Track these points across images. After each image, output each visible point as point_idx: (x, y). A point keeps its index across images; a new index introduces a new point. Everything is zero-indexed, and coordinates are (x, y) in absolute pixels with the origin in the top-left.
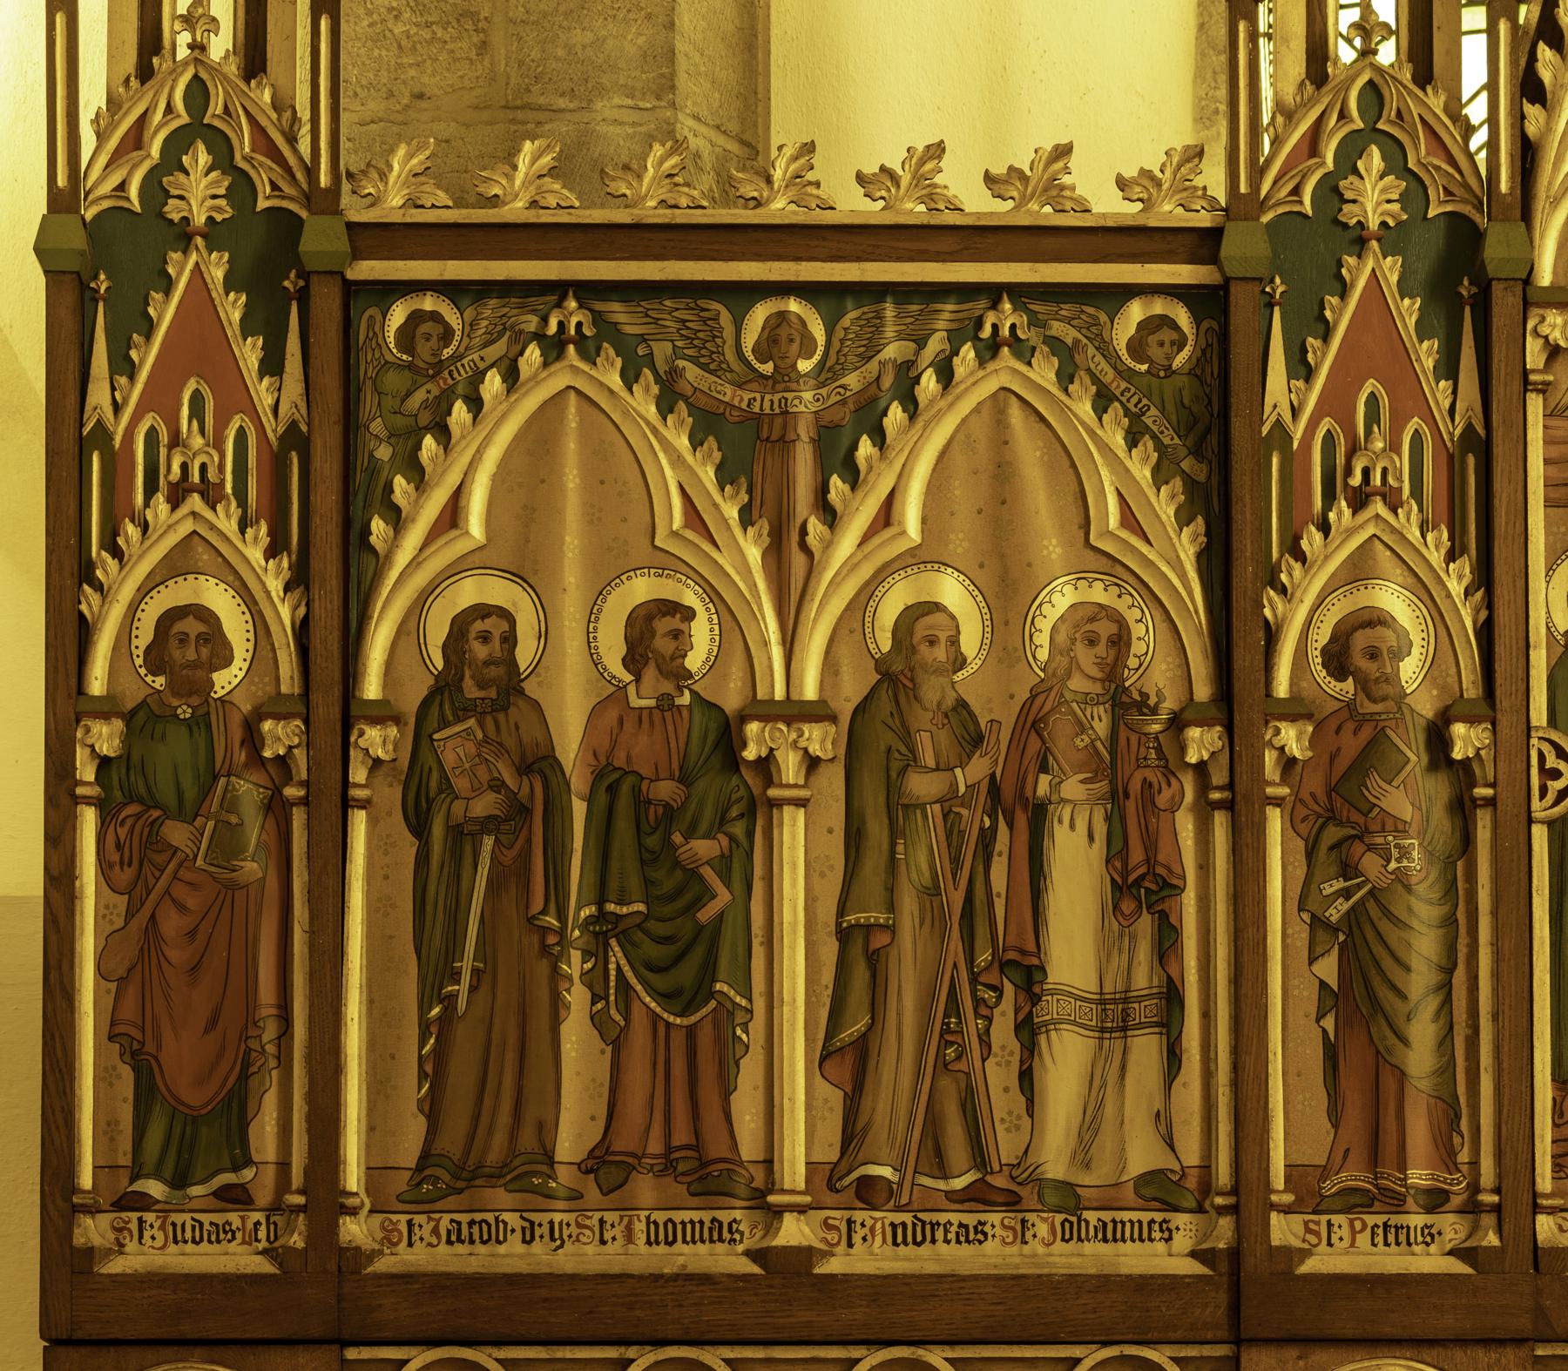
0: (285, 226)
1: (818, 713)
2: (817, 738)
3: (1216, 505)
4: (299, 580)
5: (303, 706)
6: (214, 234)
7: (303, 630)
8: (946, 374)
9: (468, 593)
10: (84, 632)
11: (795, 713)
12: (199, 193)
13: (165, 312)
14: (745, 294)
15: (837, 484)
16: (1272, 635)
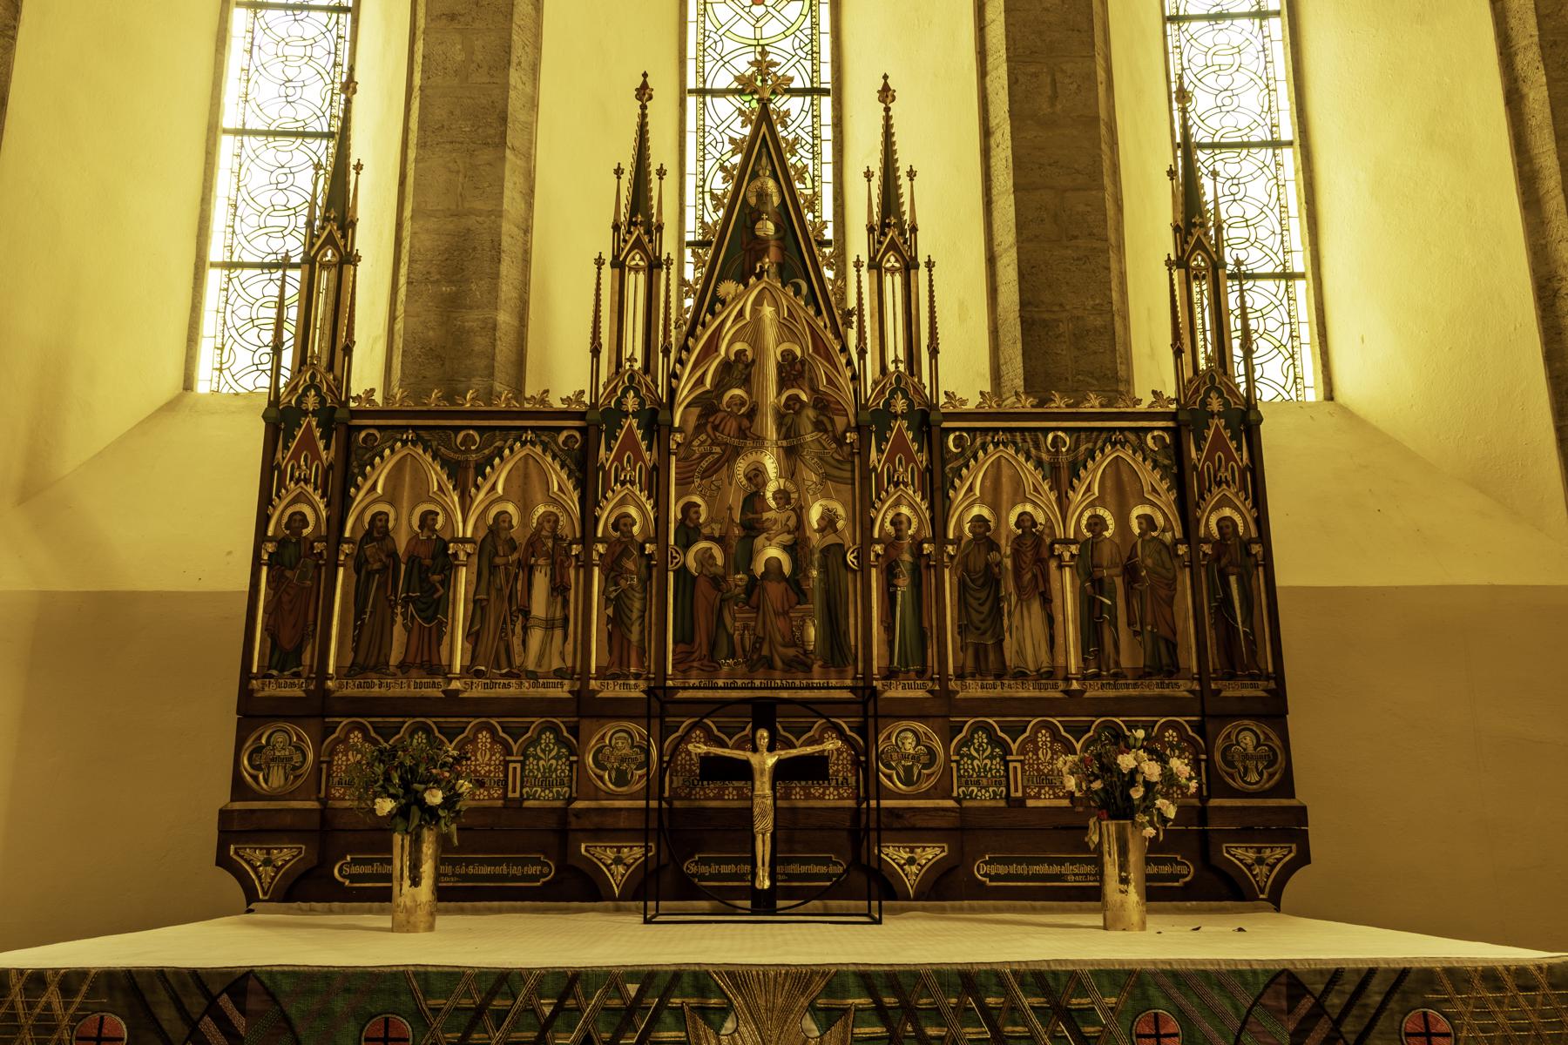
0: (925, 415)
1: (1074, 542)
2: (1074, 549)
3: (1180, 484)
4: (931, 507)
5: (932, 540)
6: (903, 416)
7: (932, 519)
8: (1102, 451)
9: (976, 511)
10: (873, 522)
11: (1067, 542)
12: (900, 405)
13: (892, 436)
14: (1046, 430)
15: (1075, 481)
16: (1198, 521)
